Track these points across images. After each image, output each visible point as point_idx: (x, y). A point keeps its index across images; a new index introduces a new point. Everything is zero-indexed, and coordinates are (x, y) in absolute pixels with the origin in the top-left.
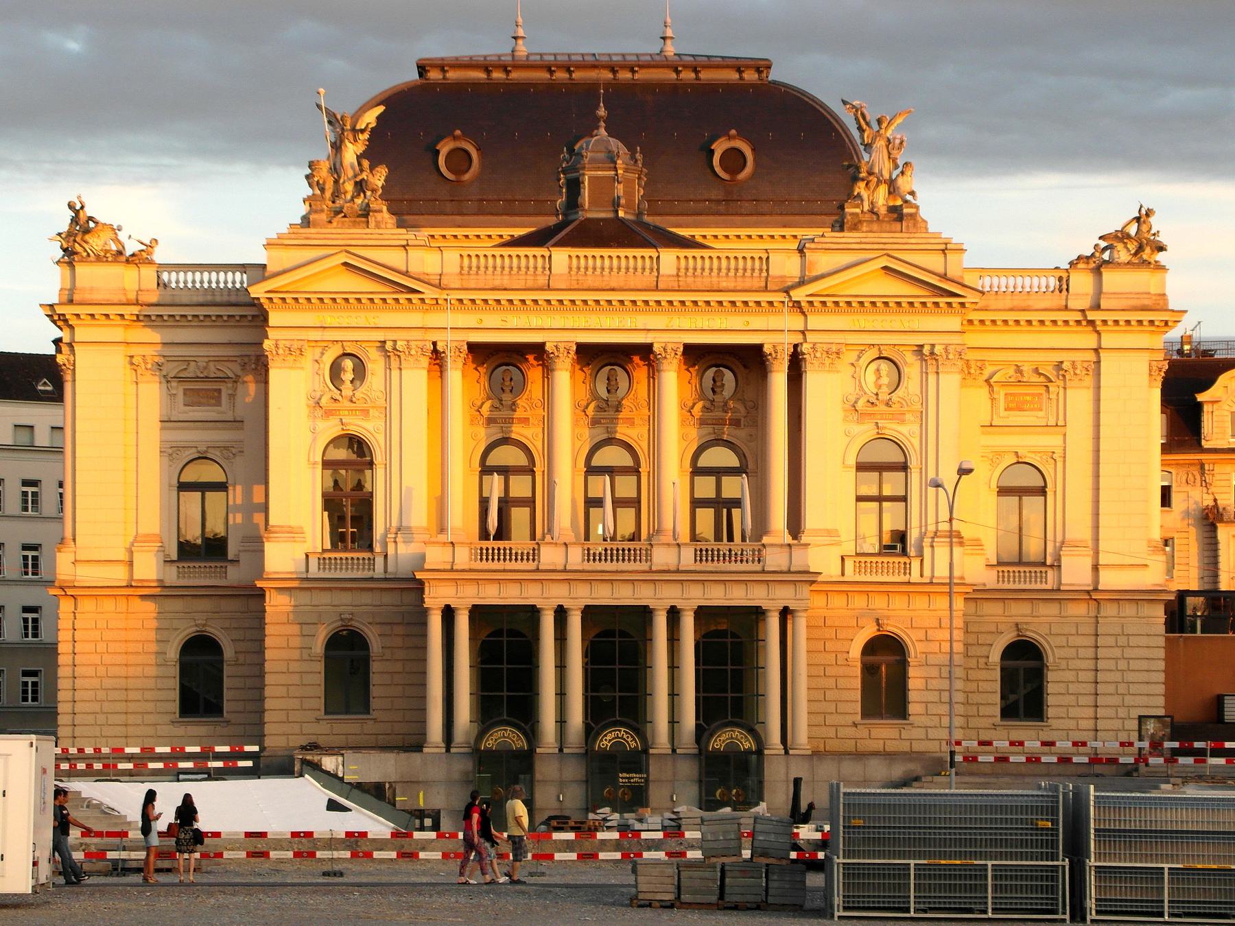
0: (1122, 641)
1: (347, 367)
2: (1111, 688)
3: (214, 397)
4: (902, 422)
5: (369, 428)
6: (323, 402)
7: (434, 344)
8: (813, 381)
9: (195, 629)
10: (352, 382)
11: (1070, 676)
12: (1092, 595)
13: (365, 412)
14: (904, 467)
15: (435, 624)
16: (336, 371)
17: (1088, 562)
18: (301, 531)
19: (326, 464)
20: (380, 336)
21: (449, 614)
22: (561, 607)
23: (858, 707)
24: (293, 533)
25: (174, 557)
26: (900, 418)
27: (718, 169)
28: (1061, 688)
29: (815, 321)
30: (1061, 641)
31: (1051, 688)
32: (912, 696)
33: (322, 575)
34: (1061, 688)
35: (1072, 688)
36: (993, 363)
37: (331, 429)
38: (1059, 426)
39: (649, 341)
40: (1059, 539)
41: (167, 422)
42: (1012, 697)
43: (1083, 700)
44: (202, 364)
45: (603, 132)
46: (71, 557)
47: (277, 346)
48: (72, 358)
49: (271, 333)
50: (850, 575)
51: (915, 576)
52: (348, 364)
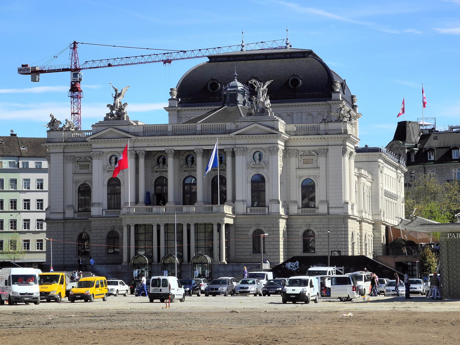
0: (336, 229)
2: (333, 243)
7: (136, 151)
8: (237, 158)
11: (322, 240)
15: (125, 230)
17: (326, 206)
18: (102, 204)
21: (129, 227)
23: (252, 250)
24: (99, 204)
27: (290, 85)
34: (319, 243)
35: (323, 243)
43: (326, 247)
45: (236, 80)
52: (113, 158)
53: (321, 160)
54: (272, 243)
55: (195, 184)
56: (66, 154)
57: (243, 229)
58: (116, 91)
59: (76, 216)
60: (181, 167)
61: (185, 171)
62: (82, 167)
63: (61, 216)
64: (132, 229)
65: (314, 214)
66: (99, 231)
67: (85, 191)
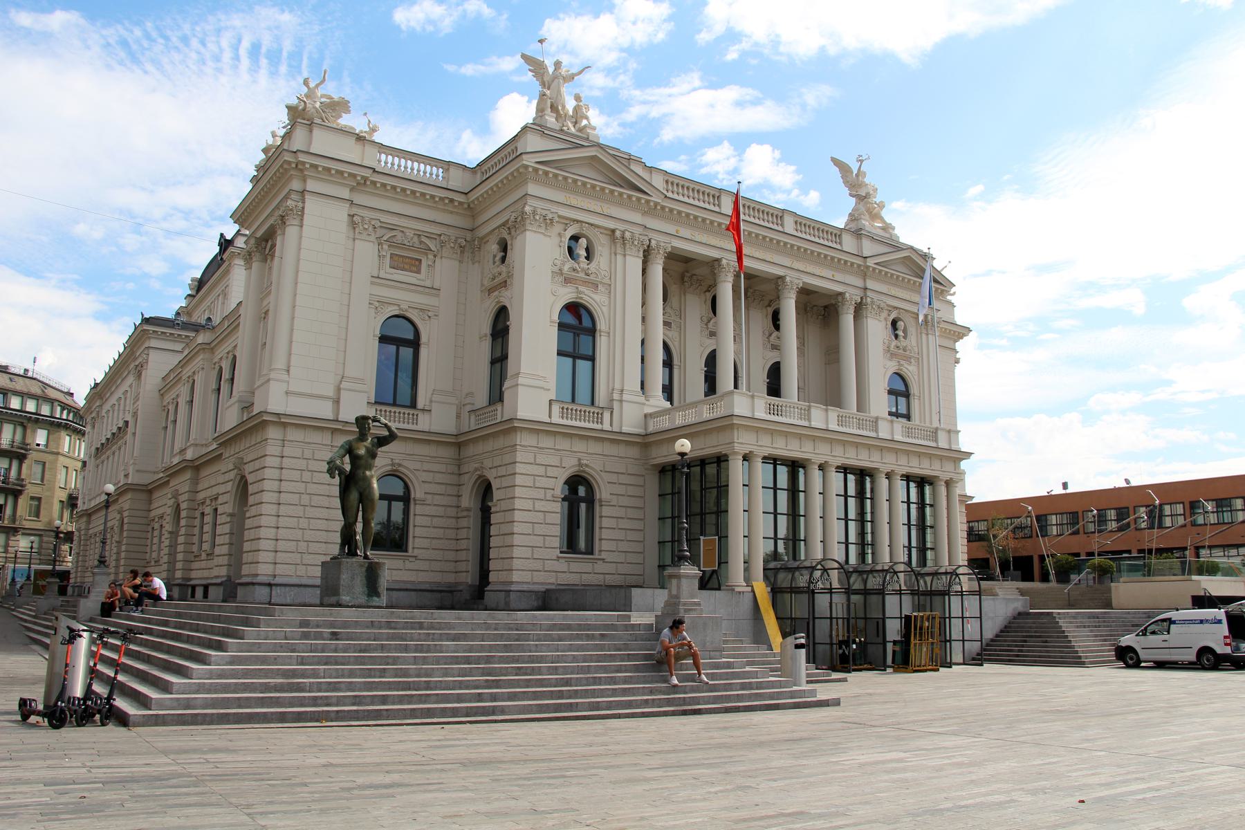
3: (415, 265)
5: (595, 300)
6: (566, 268)
9: (389, 468)
10: (587, 258)
13: (595, 286)
14: (907, 395)
20: (611, 224)
26: (908, 359)
39: (781, 274)
46: (284, 387)
47: (534, 213)
48: (300, 204)
49: (530, 201)
56: (355, 210)
62: (400, 262)
66: (541, 470)
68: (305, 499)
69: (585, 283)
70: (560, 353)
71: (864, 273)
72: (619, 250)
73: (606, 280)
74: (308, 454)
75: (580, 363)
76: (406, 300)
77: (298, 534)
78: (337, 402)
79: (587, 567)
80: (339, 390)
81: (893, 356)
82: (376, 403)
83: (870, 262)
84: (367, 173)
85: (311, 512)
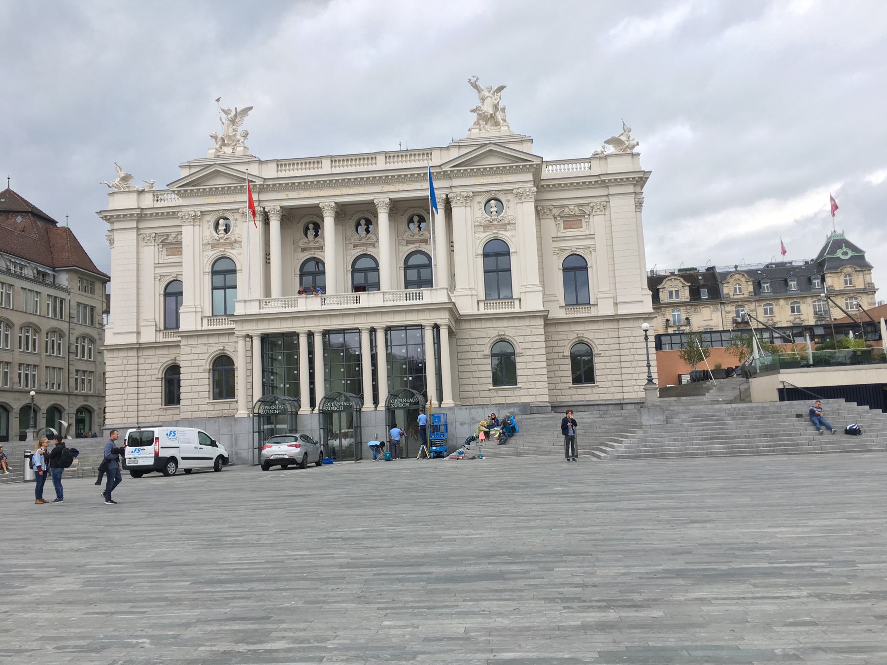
1: (222, 224)
4: (506, 230)
5: (231, 253)
8: (456, 212)
12: (615, 319)
13: (231, 244)
14: (508, 254)
16: (217, 225)
17: (611, 301)
19: (214, 273)
22: (310, 331)
23: (490, 380)
25: (162, 328)
26: (504, 226)
28: (602, 366)
29: (456, 182)
30: (601, 341)
31: (597, 366)
32: (519, 372)
33: (210, 328)
34: (602, 366)
36: (555, 207)
37: (213, 254)
38: (592, 236)
40: (596, 292)
41: (157, 265)
42: (578, 373)
44: (173, 235)
50: (482, 311)
51: (517, 309)
52: (221, 221)
53: (597, 223)
54: (530, 365)
55: (376, 269)
56: (142, 231)
57: (473, 342)
58: (226, 112)
59: (161, 338)
60: (346, 238)
61: (355, 246)
63: (132, 339)
64: (257, 343)
65: (589, 315)
66: (196, 357)
67: (173, 293)
68: (125, 385)
69: (224, 244)
70: (213, 288)
71: (447, 176)
72: (244, 220)
73: (238, 240)
74: (125, 362)
75: (227, 290)
76: (173, 271)
77: (122, 403)
78: (138, 333)
79: (227, 406)
80: (138, 325)
81: (486, 227)
82: (165, 328)
83: (447, 168)
84: (138, 211)
85: (128, 391)
